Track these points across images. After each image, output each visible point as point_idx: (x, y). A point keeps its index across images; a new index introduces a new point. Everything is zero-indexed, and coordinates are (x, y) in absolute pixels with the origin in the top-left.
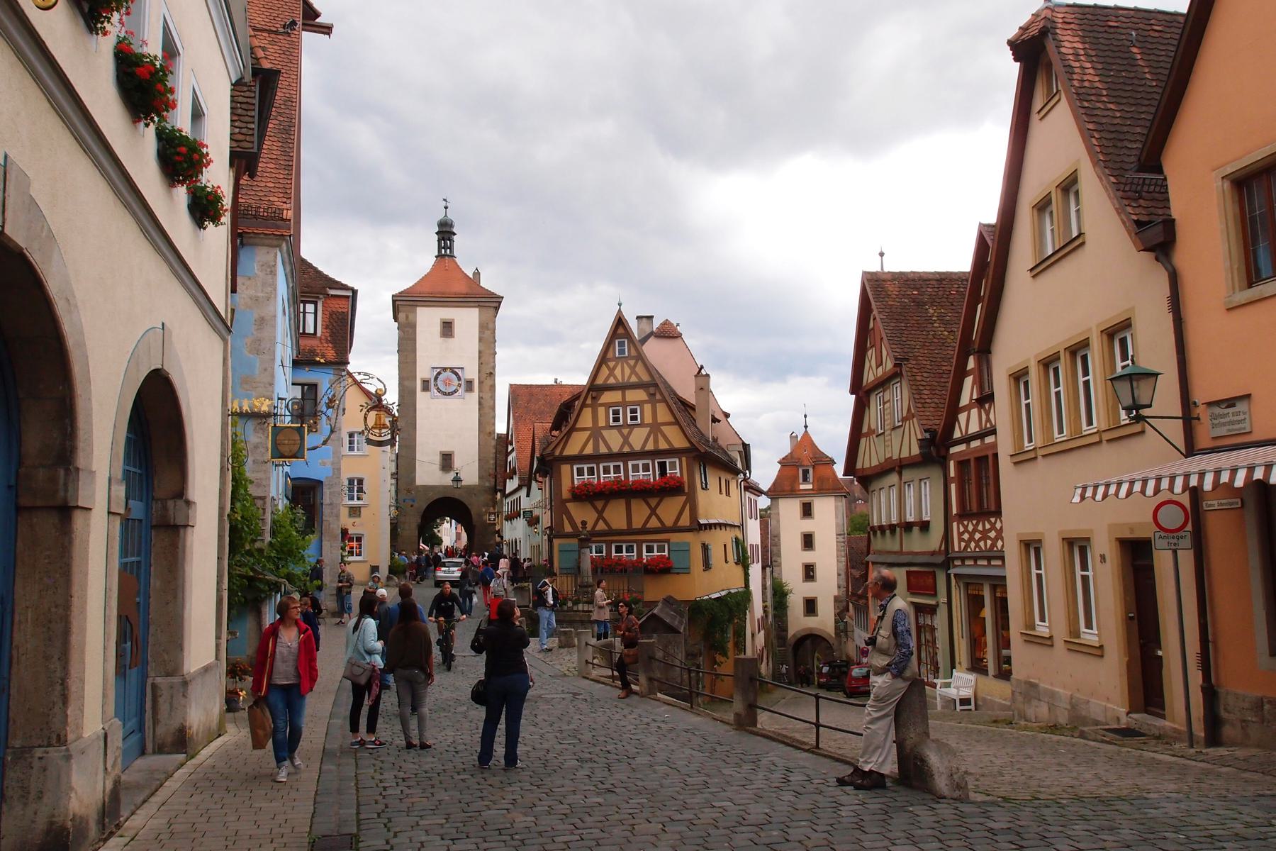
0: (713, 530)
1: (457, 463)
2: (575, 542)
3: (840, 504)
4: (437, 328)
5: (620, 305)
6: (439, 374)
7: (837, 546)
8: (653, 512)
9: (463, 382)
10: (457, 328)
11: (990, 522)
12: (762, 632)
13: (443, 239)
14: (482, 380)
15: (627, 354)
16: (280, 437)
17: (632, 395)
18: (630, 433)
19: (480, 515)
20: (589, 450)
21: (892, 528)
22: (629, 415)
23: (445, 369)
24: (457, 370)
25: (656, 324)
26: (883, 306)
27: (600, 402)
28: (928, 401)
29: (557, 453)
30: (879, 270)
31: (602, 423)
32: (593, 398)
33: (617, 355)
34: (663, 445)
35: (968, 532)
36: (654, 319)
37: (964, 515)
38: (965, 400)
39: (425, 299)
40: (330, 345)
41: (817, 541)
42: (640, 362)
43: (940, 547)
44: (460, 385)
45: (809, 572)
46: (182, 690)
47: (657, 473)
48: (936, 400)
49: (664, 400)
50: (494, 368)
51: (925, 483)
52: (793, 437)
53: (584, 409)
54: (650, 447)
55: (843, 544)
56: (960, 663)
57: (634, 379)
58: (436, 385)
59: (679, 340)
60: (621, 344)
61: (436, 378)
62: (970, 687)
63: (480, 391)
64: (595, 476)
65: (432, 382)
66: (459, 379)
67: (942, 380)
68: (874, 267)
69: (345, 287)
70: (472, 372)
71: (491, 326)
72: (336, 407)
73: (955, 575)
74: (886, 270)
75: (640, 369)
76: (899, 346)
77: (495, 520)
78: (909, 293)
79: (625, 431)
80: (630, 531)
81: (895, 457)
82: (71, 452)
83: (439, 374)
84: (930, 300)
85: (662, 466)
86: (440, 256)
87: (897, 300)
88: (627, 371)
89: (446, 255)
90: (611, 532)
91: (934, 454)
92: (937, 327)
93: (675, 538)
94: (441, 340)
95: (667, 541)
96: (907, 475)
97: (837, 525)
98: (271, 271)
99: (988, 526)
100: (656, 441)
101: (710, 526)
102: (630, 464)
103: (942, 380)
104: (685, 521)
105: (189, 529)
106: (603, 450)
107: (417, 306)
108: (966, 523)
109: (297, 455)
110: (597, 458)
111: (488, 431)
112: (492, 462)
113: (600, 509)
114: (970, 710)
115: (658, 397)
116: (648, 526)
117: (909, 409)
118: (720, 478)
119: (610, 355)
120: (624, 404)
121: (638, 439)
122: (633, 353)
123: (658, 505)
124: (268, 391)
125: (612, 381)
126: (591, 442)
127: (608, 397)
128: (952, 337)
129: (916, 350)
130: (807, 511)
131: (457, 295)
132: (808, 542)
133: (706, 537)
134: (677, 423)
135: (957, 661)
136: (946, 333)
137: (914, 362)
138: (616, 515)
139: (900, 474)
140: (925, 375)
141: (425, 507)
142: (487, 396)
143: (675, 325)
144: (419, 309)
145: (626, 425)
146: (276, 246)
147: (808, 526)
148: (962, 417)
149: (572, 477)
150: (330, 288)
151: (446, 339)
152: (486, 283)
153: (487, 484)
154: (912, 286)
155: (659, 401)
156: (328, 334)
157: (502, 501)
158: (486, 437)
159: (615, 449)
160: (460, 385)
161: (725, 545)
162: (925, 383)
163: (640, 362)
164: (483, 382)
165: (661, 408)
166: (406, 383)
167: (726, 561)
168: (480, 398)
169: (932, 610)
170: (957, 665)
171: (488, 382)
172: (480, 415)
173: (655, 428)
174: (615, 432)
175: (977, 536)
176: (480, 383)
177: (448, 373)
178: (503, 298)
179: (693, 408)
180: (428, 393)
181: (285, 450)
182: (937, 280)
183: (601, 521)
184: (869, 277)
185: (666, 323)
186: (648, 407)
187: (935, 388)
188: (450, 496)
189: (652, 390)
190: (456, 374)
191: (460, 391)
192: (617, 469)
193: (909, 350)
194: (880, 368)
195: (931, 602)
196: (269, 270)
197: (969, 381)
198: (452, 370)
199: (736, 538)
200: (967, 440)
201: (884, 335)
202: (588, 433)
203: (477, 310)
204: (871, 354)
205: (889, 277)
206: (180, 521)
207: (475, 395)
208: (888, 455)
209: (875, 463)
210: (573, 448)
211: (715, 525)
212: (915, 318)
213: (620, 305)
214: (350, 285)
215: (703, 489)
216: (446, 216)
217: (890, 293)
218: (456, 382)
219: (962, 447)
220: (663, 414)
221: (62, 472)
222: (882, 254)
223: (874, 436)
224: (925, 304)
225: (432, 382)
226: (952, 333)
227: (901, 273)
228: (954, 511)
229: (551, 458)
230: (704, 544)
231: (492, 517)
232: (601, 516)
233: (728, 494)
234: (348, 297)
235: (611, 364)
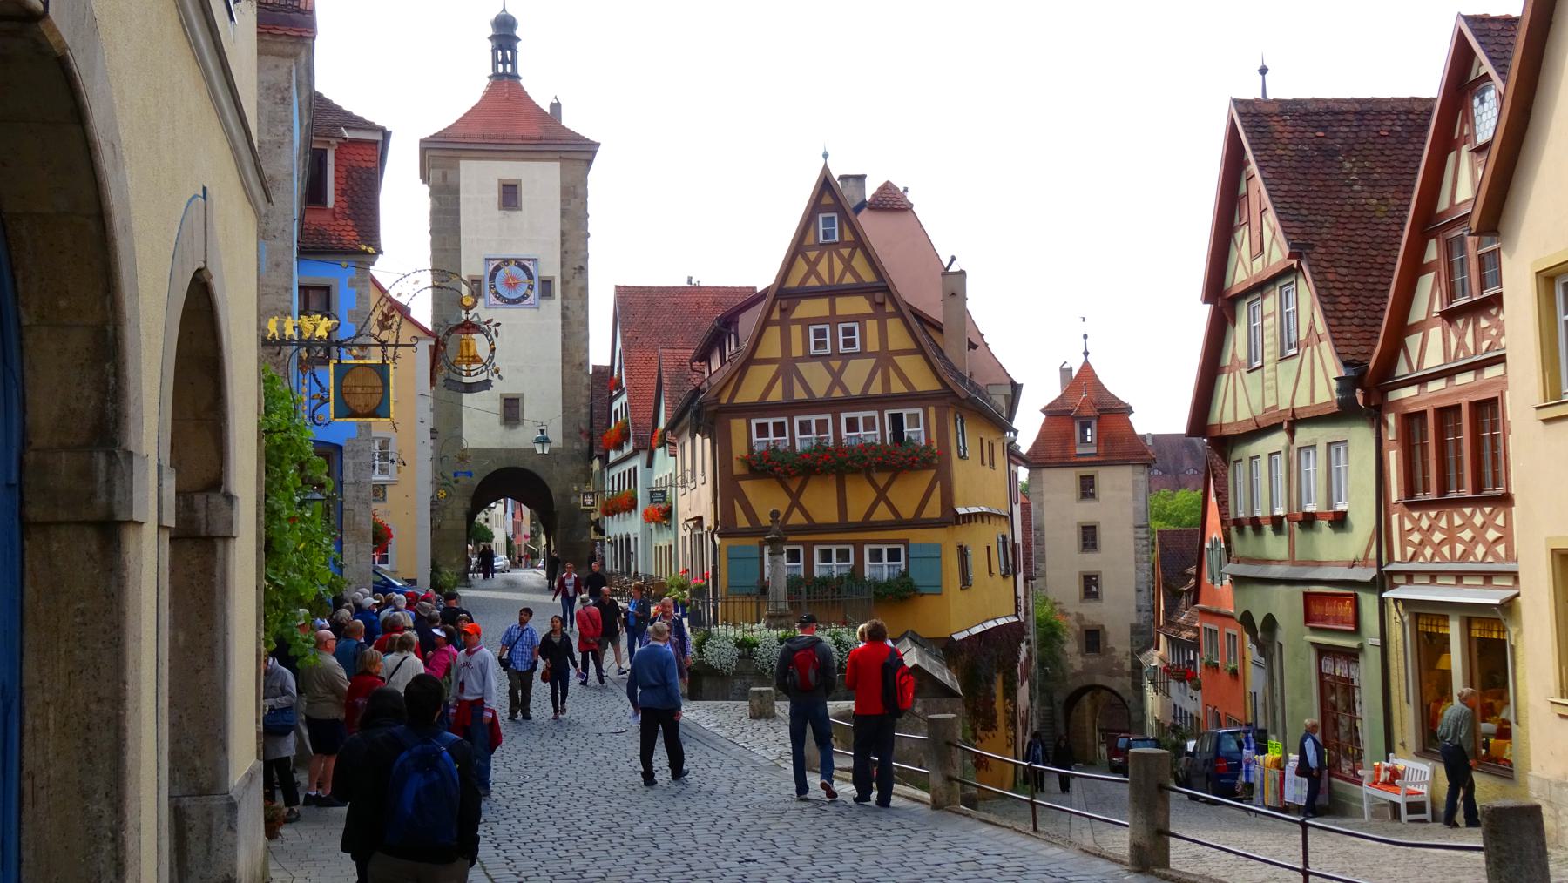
0: (973, 524)
1: (529, 411)
2: (753, 542)
3: (1142, 477)
4: (494, 195)
5: (826, 156)
6: (497, 268)
7: (1136, 545)
8: (882, 495)
9: (536, 283)
10: (525, 196)
11: (1462, 515)
12: (1026, 683)
13: (500, 47)
14: (567, 278)
15: (837, 239)
16: (348, 381)
17: (846, 306)
18: (842, 368)
19: (566, 496)
20: (776, 395)
21: (1277, 523)
22: (841, 338)
23: (507, 261)
24: (526, 263)
25: (870, 190)
26: (1267, 158)
27: (795, 315)
28: (1348, 314)
29: (724, 400)
30: (1259, 96)
31: (797, 351)
32: (782, 310)
33: (821, 240)
34: (897, 387)
35: (1420, 530)
36: (867, 180)
37: (1411, 503)
38: (1418, 313)
39: (472, 147)
40: (349, 222)
41: (1104, 536)
42: (858, 250)
43: (1368, 550)
44: (531, 287)
45: (1090, 585)
46: (226, 818)
47: (888, 432)
48: (1361, 314)
49: (899, 313)
50: (586, 258)
51: (1338, 450)
52: (1065, 372)
53: (769, 329)
54: (876, 389)
55: (1145, 542)
56: (1403, 744)
57: (849, 279)
58: (492, 287)
59: (909, 214)
60: (828, 222)
61: (493, 276)
62: (1423, 783)
63: (564, 296)
64: (787, 437)
65: (487, 283)
66: (530, 277)
67: (1370, 280)
68: (1252, 92)
69: (371, 127)
70: (550, 267)
71: (580, 190)
72: (395, 327)
73: (1396, 600)
74: (1270, 96)
75: (859, 262)
76: (1296, 224)
77: (593, 504)
78: (1308, 135)
79: (836, 364)
80: (844, 526)
81: (1285, 405)
82: (116, 423)
83: (497, 268)
84: (1346, 147)
85: (897, 420)
86: (496, 77)
87: (1291, 147)
88: (838, 266)
89: (505, 74)
90: (813, 528)
91: (1361, 402)
92: (1358, 192)
93: (918, 537)
94: (498, 214)
95: (905, 542)
96: (1304, 435)
97: (1136, 509)
98: (284, 99)
99: (1458, 521)
100: (886, 382)
101: (969, 518)
102: (844, 417)
103: (1370, 280)
104: (934, 510)
105: (232, 540)
106: (799, 394)
108: (1416, 515)
109: (379, 411)
110: (789, 407)
111: (577, 362)
112: (584, 410)
113: (794, 491)
114: (1424, 821)
115: (889, 308)
116: (872, 519)
117: (1312, 327)
118: (981, 439)
119: (810, 240)
120: (833, 319)
121: (856, 377)
122: (848, 237)
123: (888, 485)
124: (284, 301)
125: (813, 282)
126: (779, 383)
127: (807, 309)
128: (1384, 208)
129: (1324, 230)
130: (1087, 489)
131: (527, 140)
132: (1089, 537)
133: (964, 534)
134: (920, 350)
135: (1397, 740)
136: (1374, 201)
137: (1323, 251)
138: (821, 503)
139: (1292, 433)
140: (1343, 271)
141: (478, 483)
142: (574, 305)
143: (902, 190)
144: (463, 164)
145: (835, 354)
146: (290, 56)
147: (1086, 512)
148: (1413, 342)
149: (745, 436)
150: (346, 128)
151: (508, 213)
152: (569, 121)
153: (577, 446)
154: (1316, 124)
155: (892, 315)
156: (345, 205)
157: (602, 473)
159: (820, 392)
160: (531, 287)
161: (988, 548)
162: (1341, 286)
163: (858, 250)
164: (568, 282)
165: (894, 327)
167: (991, 573)
168: (564, 308)
169: (1352, 656)
170: (1397, 747)
171: (579, 283)
172: (564, 337)
173: (885, 359)
174: (818, 366)
175: (1437, 537)
176: (564, 283)
177: (513, 269)
178: (598, 145)
179: (938, 328)
181: (357, 402)
182: (1356, 113)
183: (796, 511)
184: (1243, 110)
185: (887, 187)
186: (872, 325)
187: (1358, 293)
188: (517, 465)
189: (879, 297)
190: (525, 269)
191: (532, 297)
192: (822, 426)
193: (1314, 230)
194: (1258, 262)
195: (1352, 643)
196: (279, 96)
197: (1427, 282)
198: (519, 263)
199: (1004, 537)
200: (1423, 381)
201: (1267, 203)
202: (775, 367)
203: (558, 164)
204: (1242, 236)
205: (1277, 109)
206: (121, 517)
207: (556, 303)
208: (1269, 403)
209: (1244, 414)
210: (750, 393)
211: (982, 514)
212: (1321, 177)
213: (826, 156)
214: (379, 122)
215: (961, 457)
216: (504, 10)
217: (1277, 135)
219: (1411, 391)
220: (898, 337)
221: (101, 460)
222: (1263, 71)
223: (1244, 371)
224: (1338, 152)
225: (487, 283)
226: (1383, 202)
227: (1296, 102)
228: (1394, 497)
229: (715, 408)
230: (961, 547)
231: (589, 500)
232: (796, 503)
233: (992, 464)
234: (376, 143)
235: (812, 255)
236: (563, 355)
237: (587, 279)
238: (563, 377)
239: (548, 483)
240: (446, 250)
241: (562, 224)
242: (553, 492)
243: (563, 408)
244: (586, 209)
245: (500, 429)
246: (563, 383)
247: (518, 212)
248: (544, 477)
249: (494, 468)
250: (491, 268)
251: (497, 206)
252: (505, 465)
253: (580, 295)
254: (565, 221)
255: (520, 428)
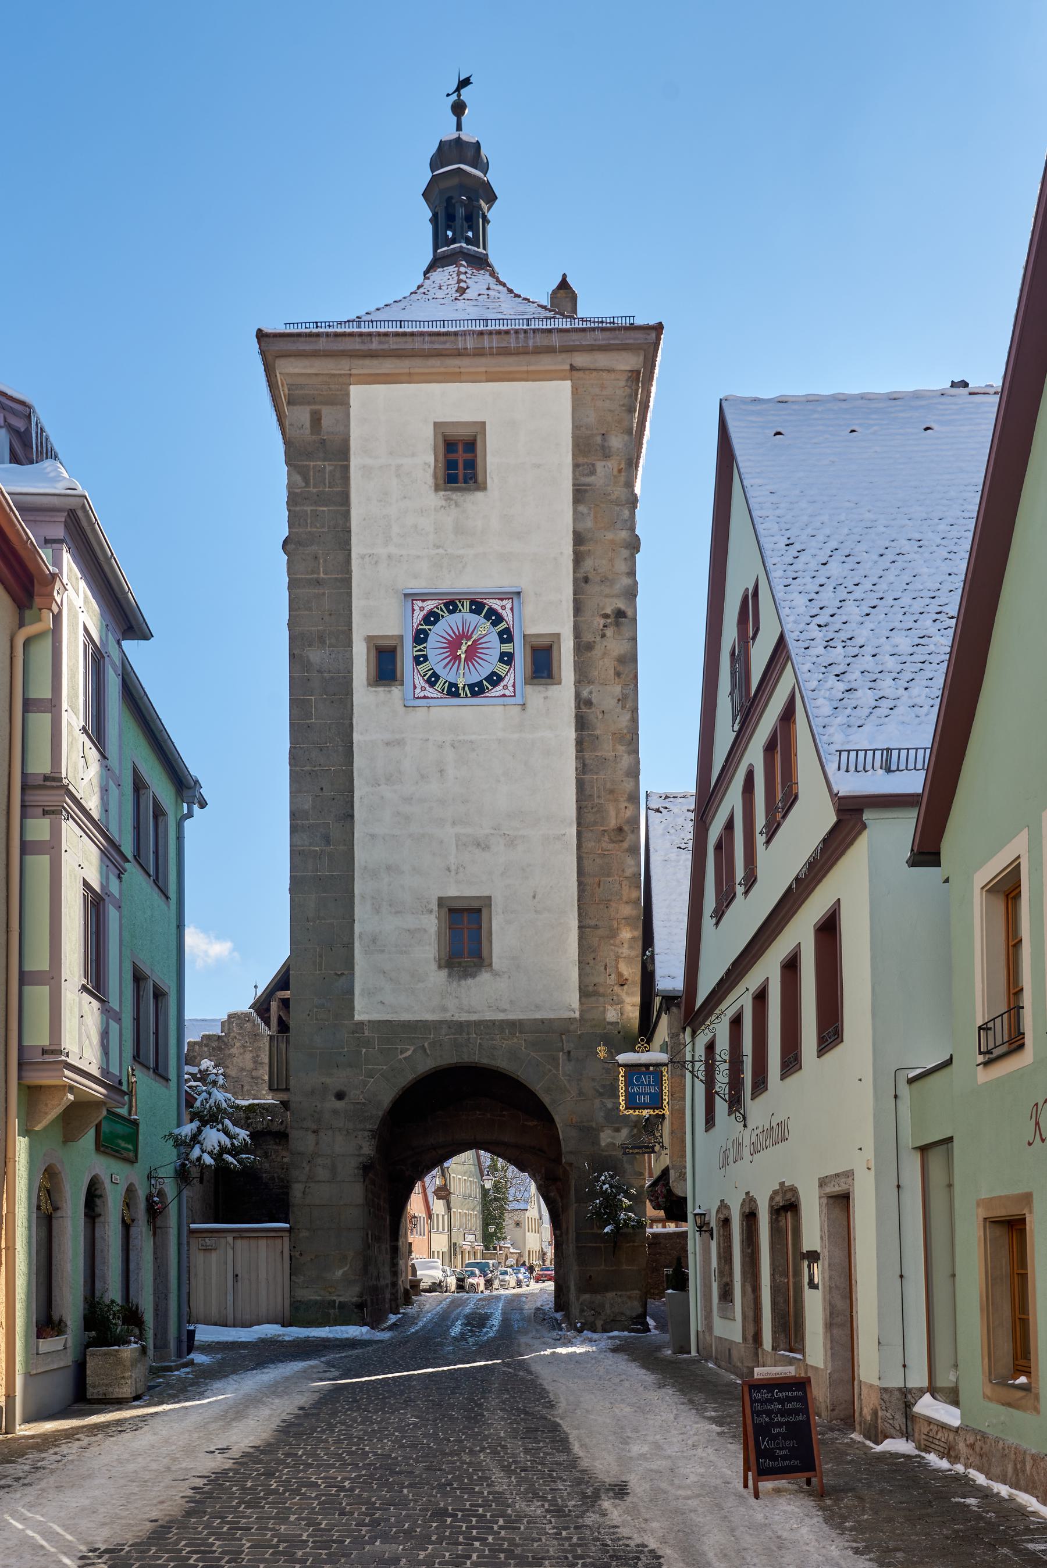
6: (432, 618)
9: (518, 649)
14: (588, 637)
24: (496, 604)
44: (507, 659)
50: (631, 593)
61: (421, 637)
65: (408, 651)
66: (506, 637)
71: (616, 442)
83: (432, 618)
94: (433, 499)
107: (349, 379)
111: (613, 823)
142: (607, 696)
151: (456, 496)
158: (606, 844)
160: (507, 659)
164: (590, 647)
166: (316, 656)
168: (582, 703)
171: (615, 646)
172: (583, 768)
176: (582, 648)
177: (465, 617)
180: (396, 691)
191: (508, 681)
203: (565, 387)
218: (493, 647)
236: (579, 809)
237: (634, 639)
238: (580, 859)
239: (546, 1100)
240: (318, 582)
241: (577, 516)
242: (557, 1118)
243: (581, 927)
244: (630, 484)
245: (438, 977)
246: (580, 872)
247: (479, 495)
248: (538, 1087)
249: (426, 1065)
250: (419, 616)
251: (430, 481)
252: (447, 1058)
253: (618, 674)
254: (582, 508)
255: (485, 976)
